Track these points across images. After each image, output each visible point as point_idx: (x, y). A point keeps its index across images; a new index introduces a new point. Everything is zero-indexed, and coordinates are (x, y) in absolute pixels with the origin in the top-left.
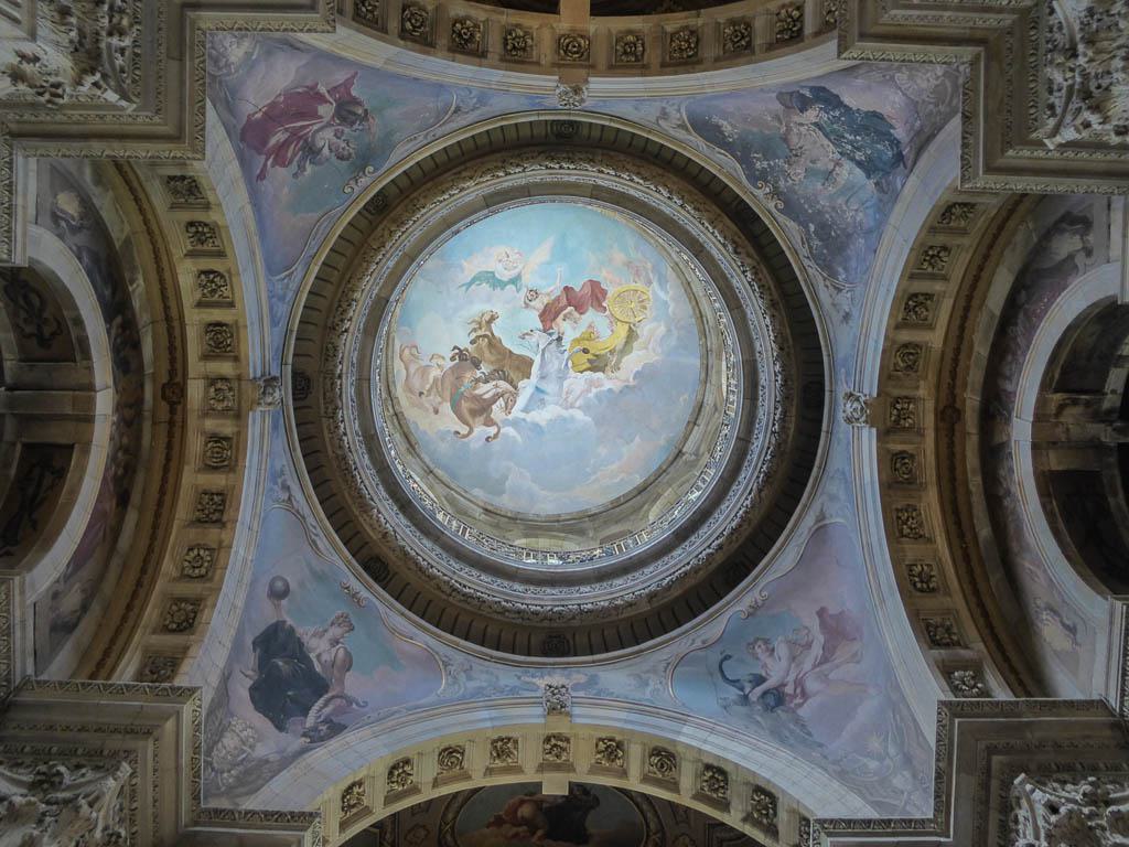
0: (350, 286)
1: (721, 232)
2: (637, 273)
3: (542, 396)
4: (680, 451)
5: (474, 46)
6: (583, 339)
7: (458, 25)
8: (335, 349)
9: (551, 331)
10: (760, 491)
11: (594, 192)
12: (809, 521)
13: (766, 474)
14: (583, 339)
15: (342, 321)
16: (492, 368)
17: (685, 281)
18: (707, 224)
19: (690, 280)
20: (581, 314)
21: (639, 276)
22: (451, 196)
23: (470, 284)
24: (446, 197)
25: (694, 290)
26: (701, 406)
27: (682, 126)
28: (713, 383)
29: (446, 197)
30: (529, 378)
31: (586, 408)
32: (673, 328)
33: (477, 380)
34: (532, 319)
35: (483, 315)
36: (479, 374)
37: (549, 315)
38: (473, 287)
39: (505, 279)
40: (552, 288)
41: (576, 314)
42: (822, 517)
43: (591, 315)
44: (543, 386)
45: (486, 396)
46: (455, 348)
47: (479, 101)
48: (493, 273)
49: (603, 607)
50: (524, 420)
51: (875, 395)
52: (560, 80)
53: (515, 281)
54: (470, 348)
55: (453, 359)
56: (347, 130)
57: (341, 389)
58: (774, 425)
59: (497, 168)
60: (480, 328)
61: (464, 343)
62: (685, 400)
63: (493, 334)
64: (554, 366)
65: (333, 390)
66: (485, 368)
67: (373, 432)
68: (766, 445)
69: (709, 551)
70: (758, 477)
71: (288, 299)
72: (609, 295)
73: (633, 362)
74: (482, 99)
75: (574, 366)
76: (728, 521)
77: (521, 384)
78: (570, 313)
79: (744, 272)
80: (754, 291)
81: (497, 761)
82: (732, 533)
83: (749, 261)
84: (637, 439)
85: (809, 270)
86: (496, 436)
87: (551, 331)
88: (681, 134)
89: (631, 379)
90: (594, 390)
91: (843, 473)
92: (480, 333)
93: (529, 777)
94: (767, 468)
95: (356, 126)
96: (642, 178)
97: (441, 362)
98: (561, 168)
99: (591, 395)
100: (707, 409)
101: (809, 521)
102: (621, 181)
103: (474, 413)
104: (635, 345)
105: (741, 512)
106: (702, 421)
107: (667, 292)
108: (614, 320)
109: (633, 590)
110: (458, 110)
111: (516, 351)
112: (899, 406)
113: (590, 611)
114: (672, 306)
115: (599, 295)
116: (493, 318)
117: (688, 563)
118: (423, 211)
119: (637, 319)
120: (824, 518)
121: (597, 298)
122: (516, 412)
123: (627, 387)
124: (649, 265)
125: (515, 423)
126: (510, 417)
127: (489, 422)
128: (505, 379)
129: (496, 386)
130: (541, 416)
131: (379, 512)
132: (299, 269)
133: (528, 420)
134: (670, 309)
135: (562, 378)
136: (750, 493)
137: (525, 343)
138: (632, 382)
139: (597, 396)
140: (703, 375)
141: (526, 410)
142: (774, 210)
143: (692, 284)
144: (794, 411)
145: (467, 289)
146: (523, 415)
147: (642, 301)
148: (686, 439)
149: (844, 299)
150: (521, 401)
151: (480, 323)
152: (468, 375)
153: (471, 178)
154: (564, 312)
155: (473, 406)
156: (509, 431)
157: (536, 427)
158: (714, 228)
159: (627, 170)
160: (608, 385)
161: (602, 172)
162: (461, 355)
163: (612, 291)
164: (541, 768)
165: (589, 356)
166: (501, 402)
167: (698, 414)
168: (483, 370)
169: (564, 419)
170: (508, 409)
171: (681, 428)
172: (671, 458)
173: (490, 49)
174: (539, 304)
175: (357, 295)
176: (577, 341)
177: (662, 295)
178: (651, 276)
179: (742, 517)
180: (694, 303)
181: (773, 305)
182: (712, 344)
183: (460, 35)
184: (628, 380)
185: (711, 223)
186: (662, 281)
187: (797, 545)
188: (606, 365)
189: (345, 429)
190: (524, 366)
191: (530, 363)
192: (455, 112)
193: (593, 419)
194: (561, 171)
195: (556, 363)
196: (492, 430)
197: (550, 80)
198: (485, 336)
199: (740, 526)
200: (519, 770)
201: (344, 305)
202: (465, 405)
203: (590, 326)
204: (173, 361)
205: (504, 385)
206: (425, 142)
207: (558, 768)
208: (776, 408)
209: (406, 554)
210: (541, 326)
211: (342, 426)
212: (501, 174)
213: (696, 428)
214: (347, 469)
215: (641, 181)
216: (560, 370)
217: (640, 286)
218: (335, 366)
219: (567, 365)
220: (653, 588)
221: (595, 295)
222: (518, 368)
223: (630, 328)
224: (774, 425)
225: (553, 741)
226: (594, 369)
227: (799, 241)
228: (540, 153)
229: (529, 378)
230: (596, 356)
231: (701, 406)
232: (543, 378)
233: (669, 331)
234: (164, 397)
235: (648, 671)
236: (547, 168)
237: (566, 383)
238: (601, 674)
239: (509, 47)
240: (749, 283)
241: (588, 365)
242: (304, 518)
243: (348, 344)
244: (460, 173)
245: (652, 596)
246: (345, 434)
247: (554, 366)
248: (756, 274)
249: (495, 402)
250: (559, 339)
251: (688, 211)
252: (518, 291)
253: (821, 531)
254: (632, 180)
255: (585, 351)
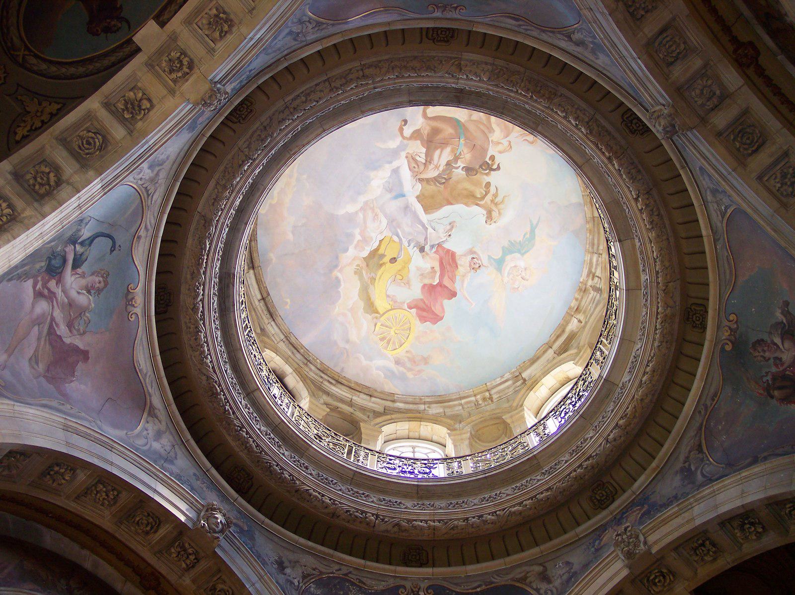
0: (664, 238)
1: (422, 528)
2: (413, 361)
3: (394, 194)
4: (253, 268)
5: (736, 523)
6: (404, 267)
7: (760, 530)
8: (633, 178)
9: (434, 250)
10: (209, 378)
11: (535, 462)
12: (156, 401)
13: (218, 394)
14: (404, 267)
15: (647, 205)
16: (454, 178)
17: (376, 394)
18: (437, 524)
19: (373, 399)
20: (425, 285)
21: (408, 357)
22: (645, 373)
23: (532, 231)
24: (648, 369)
25: (362, 396)
26: (272, 315)
27: (523, 580)
28: (282, 344)
29: (648, 369)
30: (417, 197)
31: (351, 218)
32: (347, 347)
33: (456, 159)
34: (457, 245)
35: (500, 213)
36: (460, 164)
37: (448, 261)
38: (528, 229)
39: (508, 258)
40: (465, 286)
41: (427, 281)
42: (152, 413)
43: (415, 292)
44: (400, 202)
45: (438, 152)
46: (498, 168)
47: (689, 469)
48: (523, 254)
49: (235, 178)
50: (390, 162)
51: (218, 551)
52: (648, 552)
53: (499, 264)
54: (487, 179)
55: (492, 158)
56: (774, 370)
57: (601, 150)
58: (247, 433)
59: (628, 424)
60: (492, 201)
61: (494, 178)
62: (287, 303)
63: (477, 205)
64: (406, 224)
65: (608, 146)
66: (459, 172)
67: (540, 128)
68: (238, 414)
69: (201, 297)
70: (220, 385)
71: (708, 193)
72: (418, 322)
73: (350, 289)
74: (687, 474)
75: (391, 240)
76: (208, 334)
77: (419, 187)
78: (433, 278)
79: (377, 516)
80: (357, 510)
81: (214, 11)
82: (196, 327)
83: (383, 527)
84: (290, 237)
85: (337, 567)
86: (401, 130)
87: (434, 250)
88: (518, 574)
89: (339, 275)
90: (358, 237)
91: (171, 462)
92: (489, 197)
93: (176, 23)
94: (221, 398)
95: (769, 378)
96: (514, 512)
97: (500, 148)
98: (580, 466)
99: (357, 232)
100: (266, 319)
101: (156, 401)
102: (528, 496)
103: (435, 131)
104: (362, 304)
105: (206, 349)
106: (260, 306)
107: (378, 368)
108: (396, 305)
109: (225, 211)
110: (699, 449)
111: (447, 209)
112: (192, 557)
113: (241, 166)
114: (365, 362)
115: (425, 314)
116: (489, 217)
117: (205, 273)
118: (656, 344)
119: (379, 324)
120: (149, 414)
121: (424, 310)
122: (402, 163)
123: (336, 266)
124: (410, 375)
125: (395, 153)
126: (403, 154)
127: (416, 135)
128: (435, 179)
129: (437, 167)
130: (379, 180)
131: (481, 81)
132: (719, 224)
133: (387, 166)
134: (362, 358)
135: (392, 223)
136: (213, 367)
137: (446, 222)
138: (336, 273)
139: (350, 236)
140: (293, 340)
141: (396, 171)
142: (403, 583)
143: (368, 398)
144: (243, 455)
145: (531, 224)
146: (395, 164)
147: (388, 342)
148: (259, 281)
149: (294, 574)
150: (406, 174)
151: (496, 204)
152: (468, 156)
153: (642, 400)
154: (438, 274)
155: (440, 136)
156: (394, 144)
157: (373, 165)
158: (429, 527)
159: (530, 509)
160: (351, 252)
161: (547, 490)
162: (489, 167)
163: (418, 327)
164: (174, 38)
165: (387, 259)
166: (422, 159)
167: (267, 307)
168: (459, 171)
169: (359, 193)
170: (412, 159)
171: (268, 281)
172: (255, 255)
173: (720, 532)
174: (463, 263)
175: (652, 235)
176: (410, 260)
177: (380, 362)
178: (401, 369)
179: (202, 346)
180: (352, 385)
181: (334, 515)
182: (311, 370)
183: (752, 524)
184: (340, 271)
185: (435, 528)
186: (390, 374)
187: (146, 375)
188: (367, 266)
189: (570, 122)
190: (429, 203)
191: (427, 209)
192: (700, 446)
193: (337, 215)
194: (577, 464)
195: (407, 229)
196: (408, 131)
197: (655, 543)
198: (483, 198)
199: (197, 339)
200: (188, 22)
201: (656, 218)
202: (449, 130)
203: (408, 283)
204: (768, 81)
205: (432, 173)
206: (702, 402)
207: (160, 52)
208: (258, 446)
209: (429, 68)
210: (446, 246)
211: (574, 123)
212: (621, 422)
213: (259, 297)
214: (539, 92)
215: (513, 509)
216: (399, 227)
217: (401, 352)
218: (620, 165)
219: (398, 236)
220: (212, 229)
221: (427, 312)
222: (432, 197)
223: (377, 312)
224: (247, 433)
225: (186, 70)
226: (374, 253)
227: (364, 580)
228: (606, 462)
229: (417, 197)
230: (381, 265)
231: (272, 316)
232: (407, 208)
233: (348, 341)
234: (751, 43)
235: (157, 174)
236: (591, 456)
237: (384, 222)
238: (191, 134)
239: (708, 542)
240: (366, 513)
241: (381, 251)
242: (544, 31)
243: (626, 190)
244: (653, 395)
245: (207, 222)
246: (565, 118)
247: (406, 224)
248: (368, 524)
249: (427, 155)
250: (422, 250)
251: (459, 519)
252: (490, 257)
253: (141, 404)
254: (520, 504)
255: (393, 260)
